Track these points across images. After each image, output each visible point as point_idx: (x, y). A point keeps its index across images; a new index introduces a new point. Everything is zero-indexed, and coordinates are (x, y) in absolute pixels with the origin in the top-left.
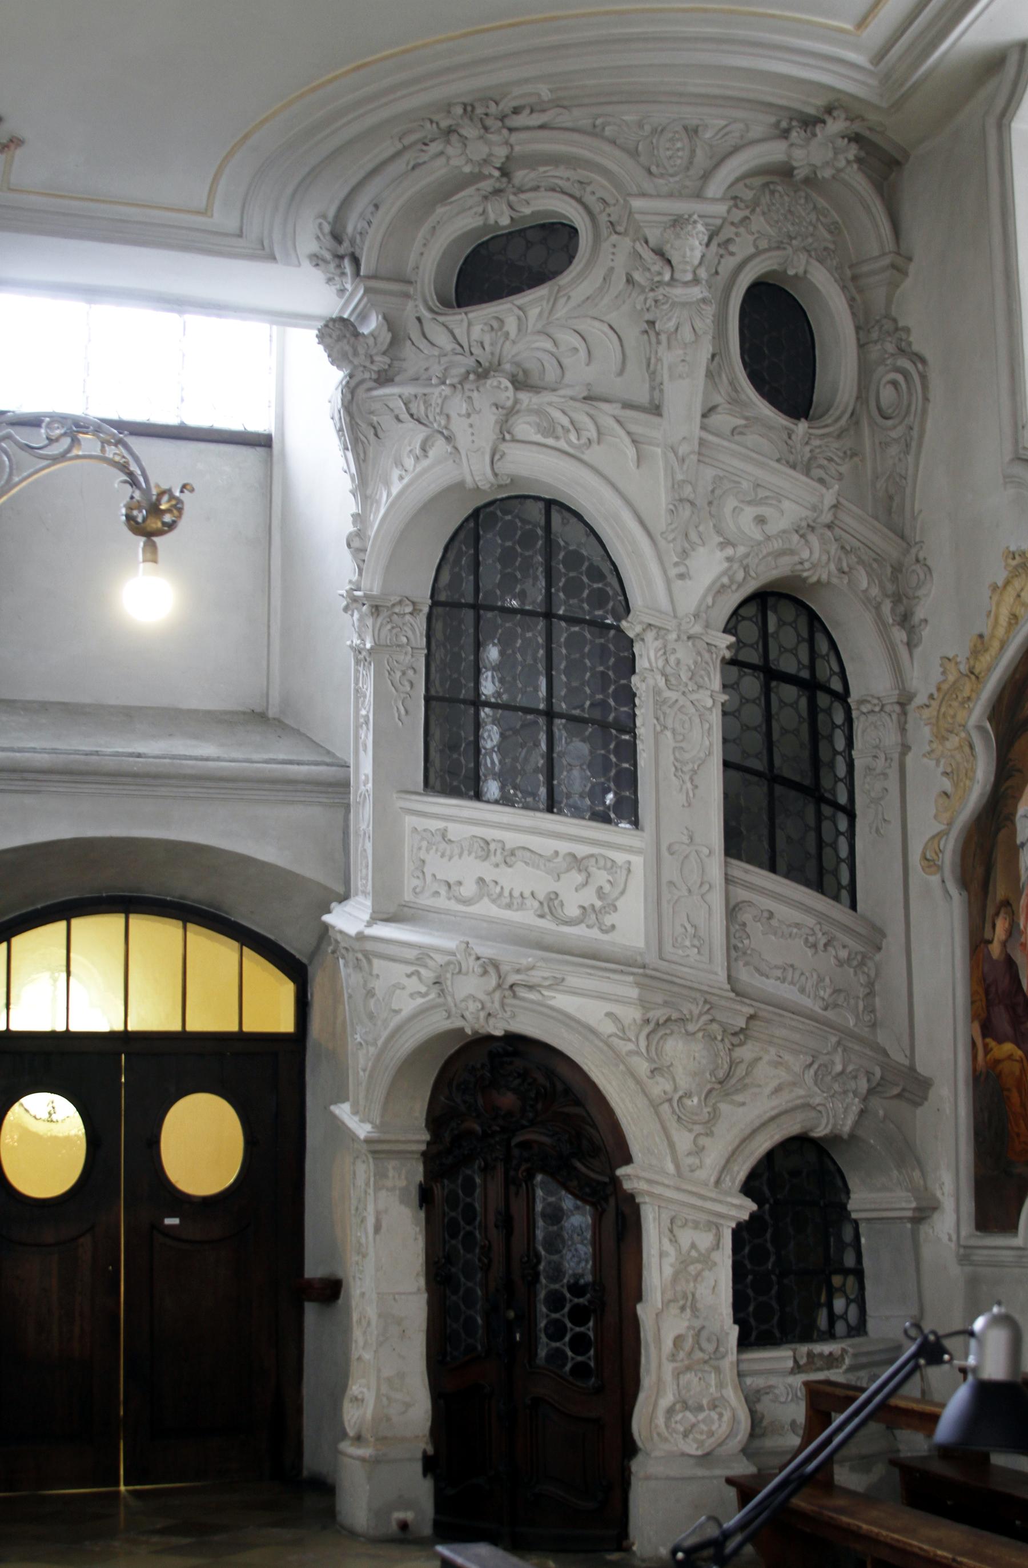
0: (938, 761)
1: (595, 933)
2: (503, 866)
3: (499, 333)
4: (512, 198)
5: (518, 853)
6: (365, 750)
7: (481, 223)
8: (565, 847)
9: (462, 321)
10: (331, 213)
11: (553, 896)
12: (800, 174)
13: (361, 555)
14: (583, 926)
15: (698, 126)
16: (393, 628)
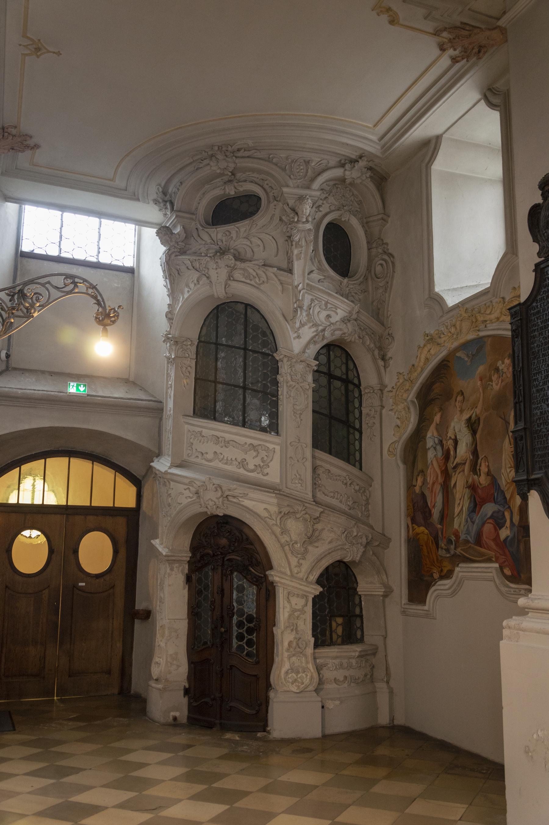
0: (395, 413)
1: (260, 476)
2: (224, 447)
4: (236, 184)
5: (230, 442)
6: (170, 398)
7: (223, 193)
8: (249, 441)
9: (214, 231)
10: (163, 184)
11: (244, 460)
12: (348, 181)
13: (171, 321)
14: (256, 473)
15: (309, 161)
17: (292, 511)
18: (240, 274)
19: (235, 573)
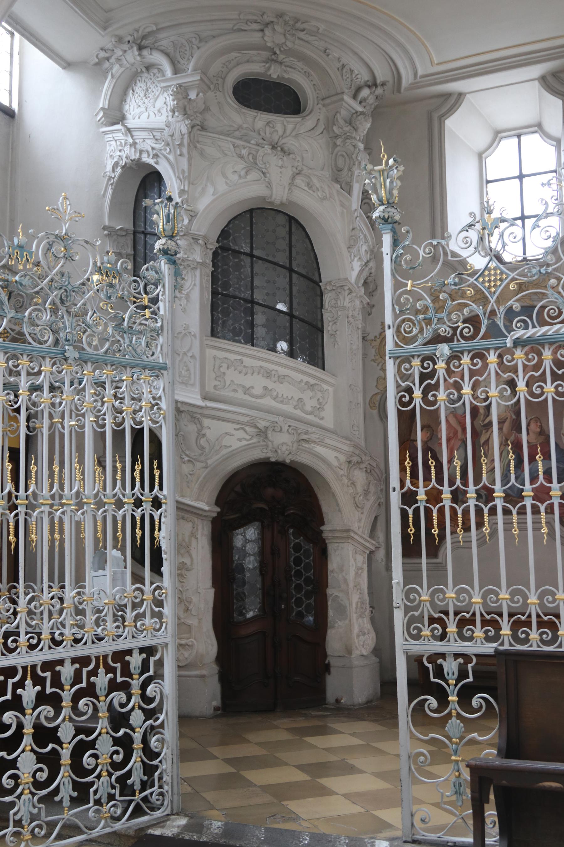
8: (306, 379)
17: (360, 460)
18: (302, 180)
19: (291, 531)
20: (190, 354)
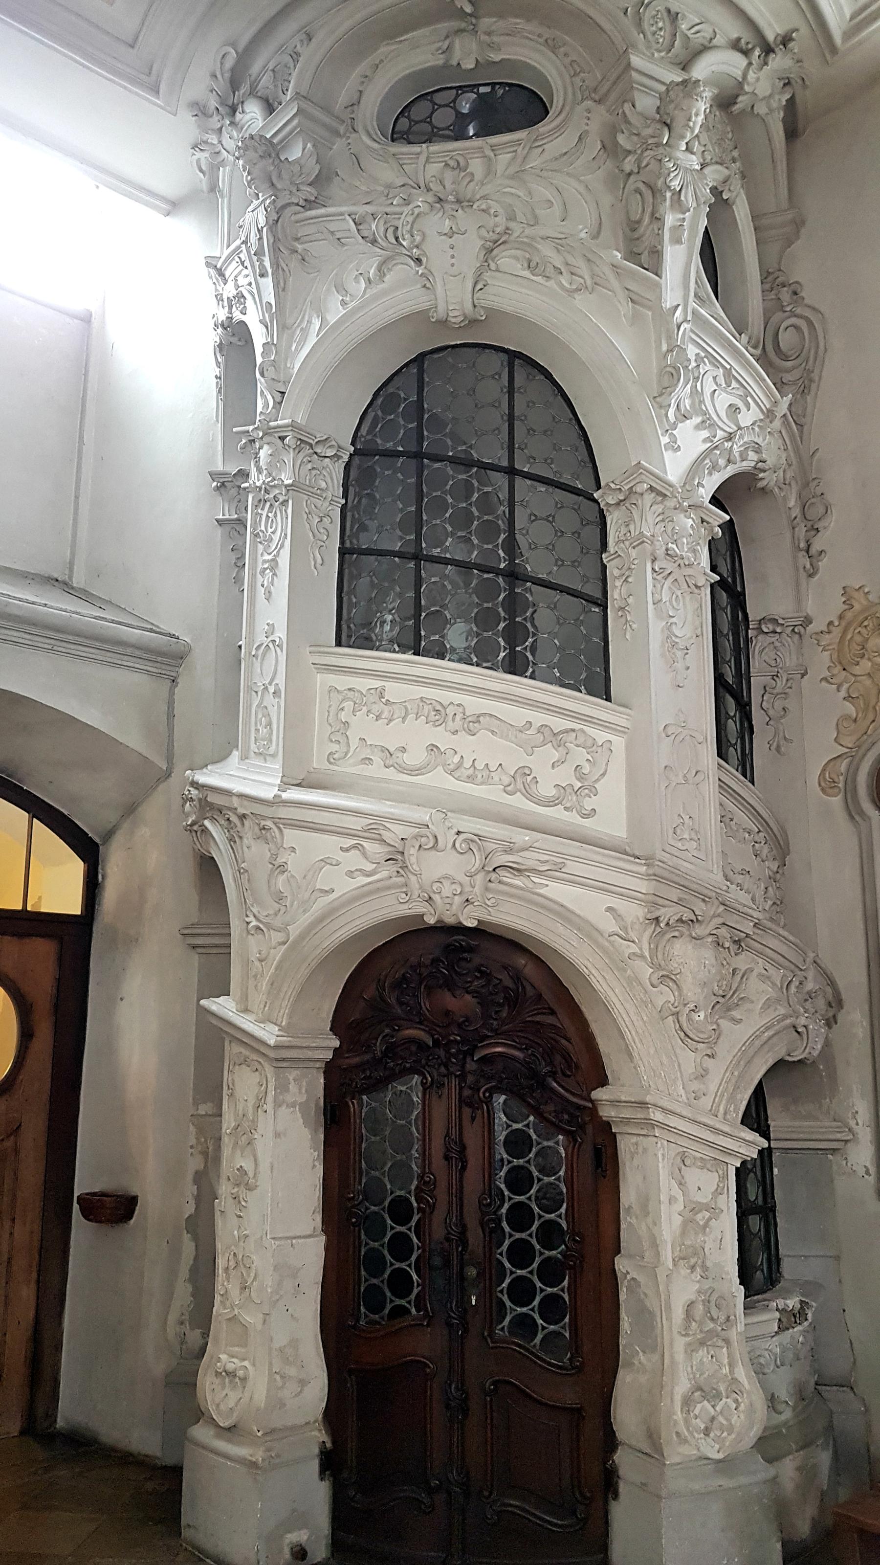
1: (573, 818)
3: (463, 174)
5: (481, 719)
8: (539, 718)
16: (314, 468)
17: (687, 915)
20: (271, 689)
